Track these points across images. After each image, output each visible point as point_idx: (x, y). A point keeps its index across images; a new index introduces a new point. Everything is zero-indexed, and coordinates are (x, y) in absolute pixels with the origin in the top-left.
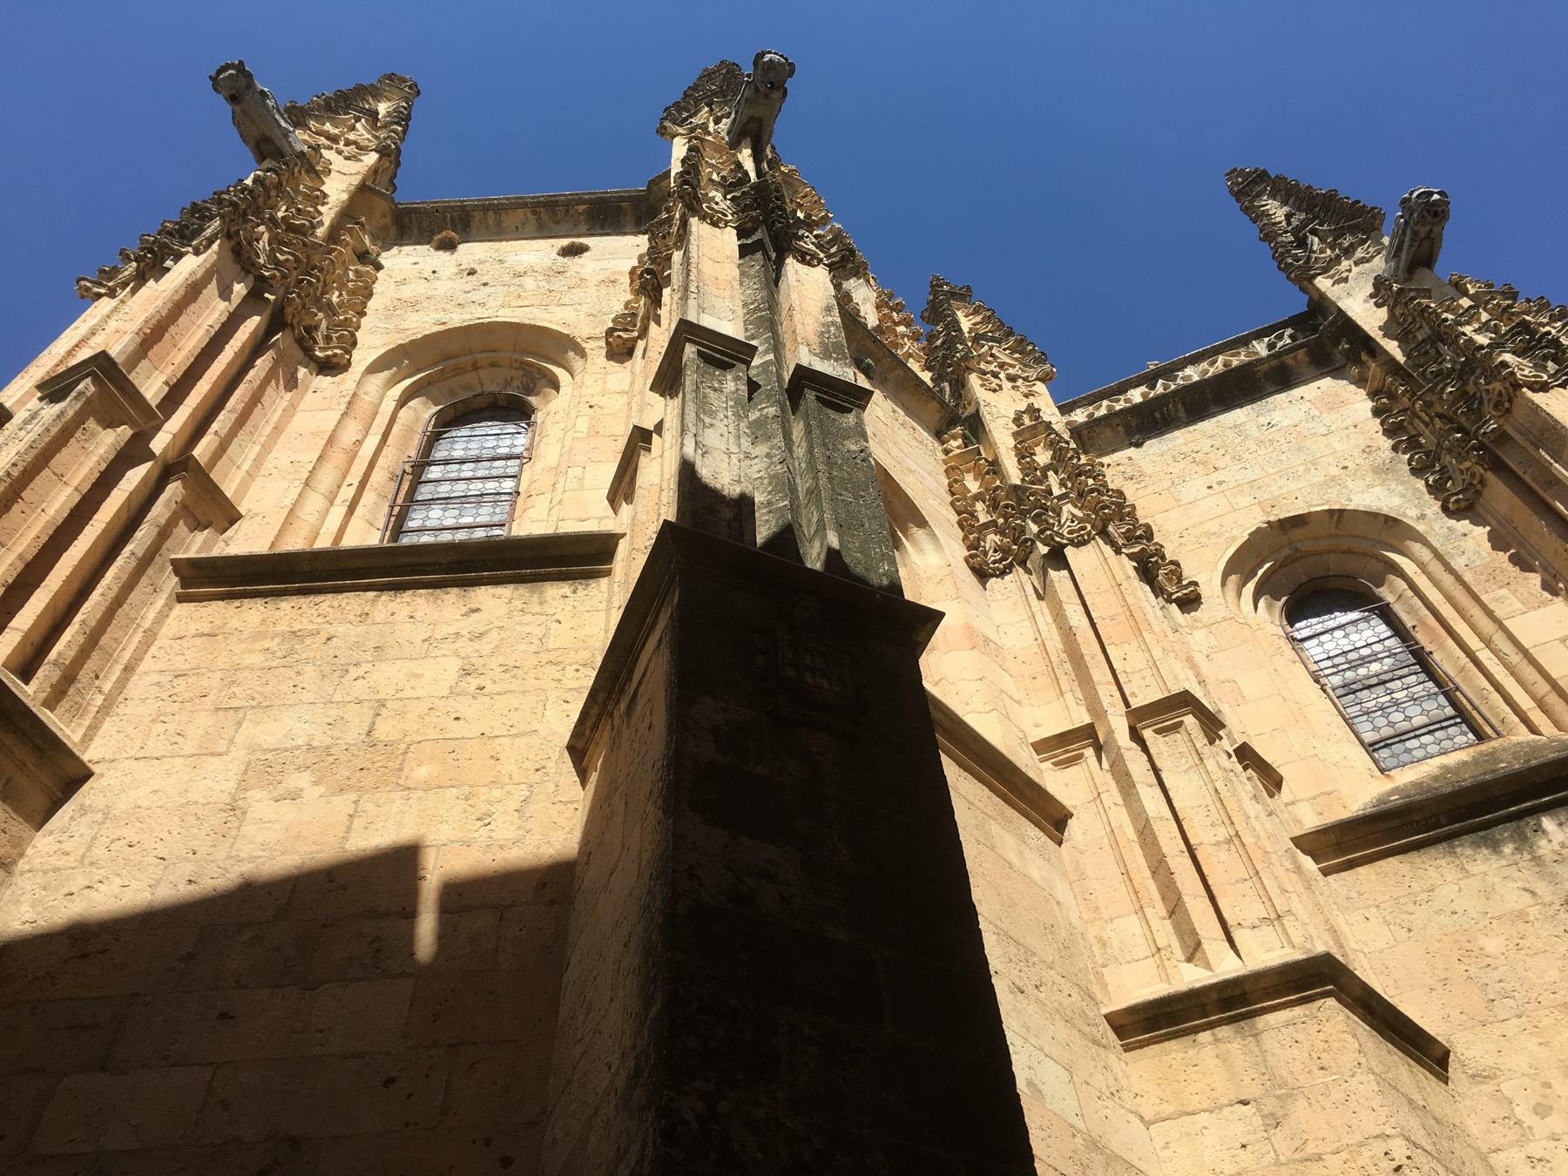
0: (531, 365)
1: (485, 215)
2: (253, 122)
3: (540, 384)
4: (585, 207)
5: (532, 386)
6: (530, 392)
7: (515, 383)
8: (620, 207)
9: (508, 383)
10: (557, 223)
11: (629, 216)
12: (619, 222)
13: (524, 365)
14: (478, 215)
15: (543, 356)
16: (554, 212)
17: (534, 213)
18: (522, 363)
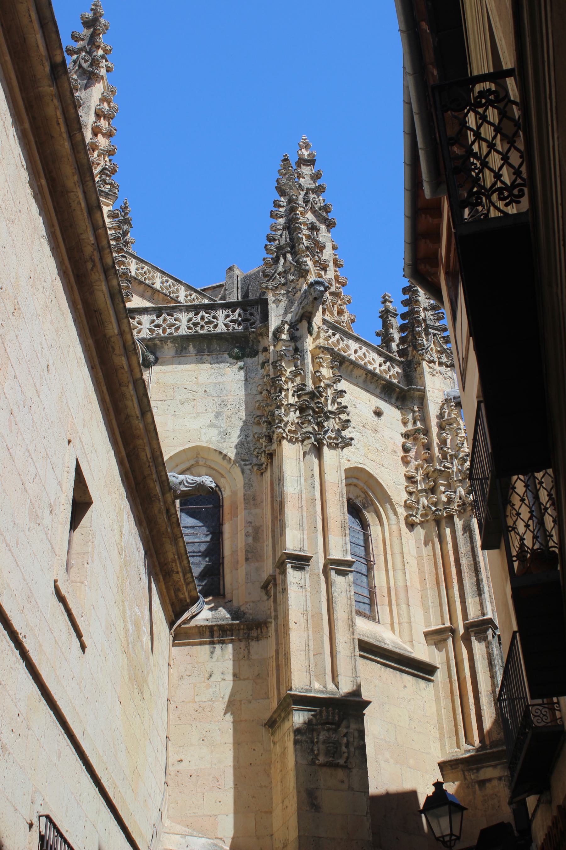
0: (369, 496)
1: (350, 365)
2: (313, 307)
3: (371, 508)
4: (384, 382)
5: (366, 505)
6: (365, 508)
7: (360, 499)
8: (395, 390)
9: (357, 497)
10: (371, 383)
11: (395, 394)
12: (391, 395)
13: (365, 493)
14: (347, 363)
15: (374, 494)
16: (373, 378)
17: (366, 374)
18: (366, 492)
